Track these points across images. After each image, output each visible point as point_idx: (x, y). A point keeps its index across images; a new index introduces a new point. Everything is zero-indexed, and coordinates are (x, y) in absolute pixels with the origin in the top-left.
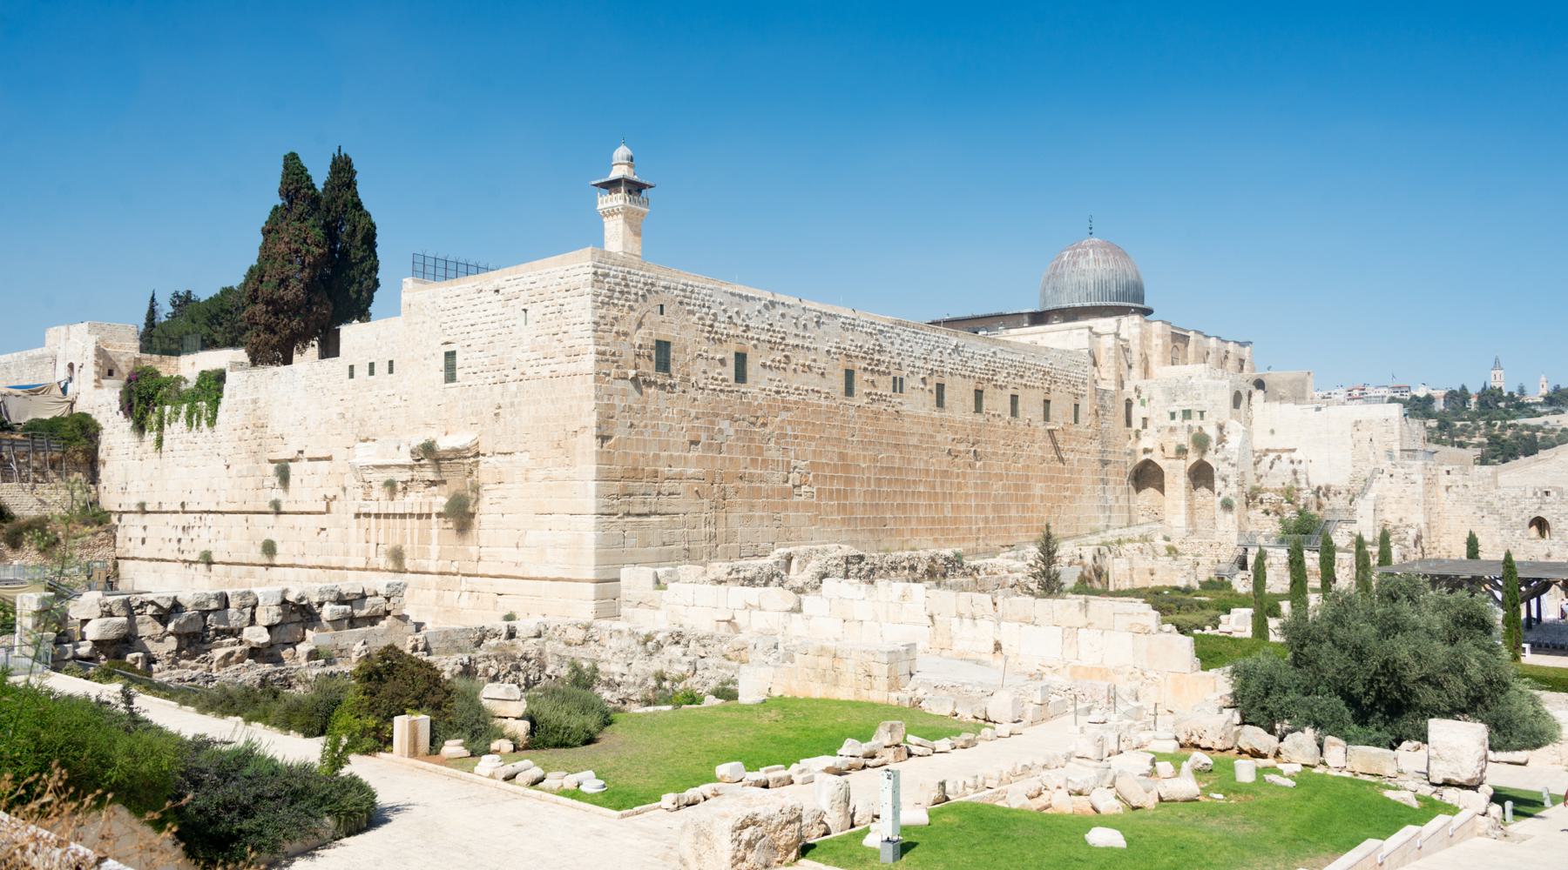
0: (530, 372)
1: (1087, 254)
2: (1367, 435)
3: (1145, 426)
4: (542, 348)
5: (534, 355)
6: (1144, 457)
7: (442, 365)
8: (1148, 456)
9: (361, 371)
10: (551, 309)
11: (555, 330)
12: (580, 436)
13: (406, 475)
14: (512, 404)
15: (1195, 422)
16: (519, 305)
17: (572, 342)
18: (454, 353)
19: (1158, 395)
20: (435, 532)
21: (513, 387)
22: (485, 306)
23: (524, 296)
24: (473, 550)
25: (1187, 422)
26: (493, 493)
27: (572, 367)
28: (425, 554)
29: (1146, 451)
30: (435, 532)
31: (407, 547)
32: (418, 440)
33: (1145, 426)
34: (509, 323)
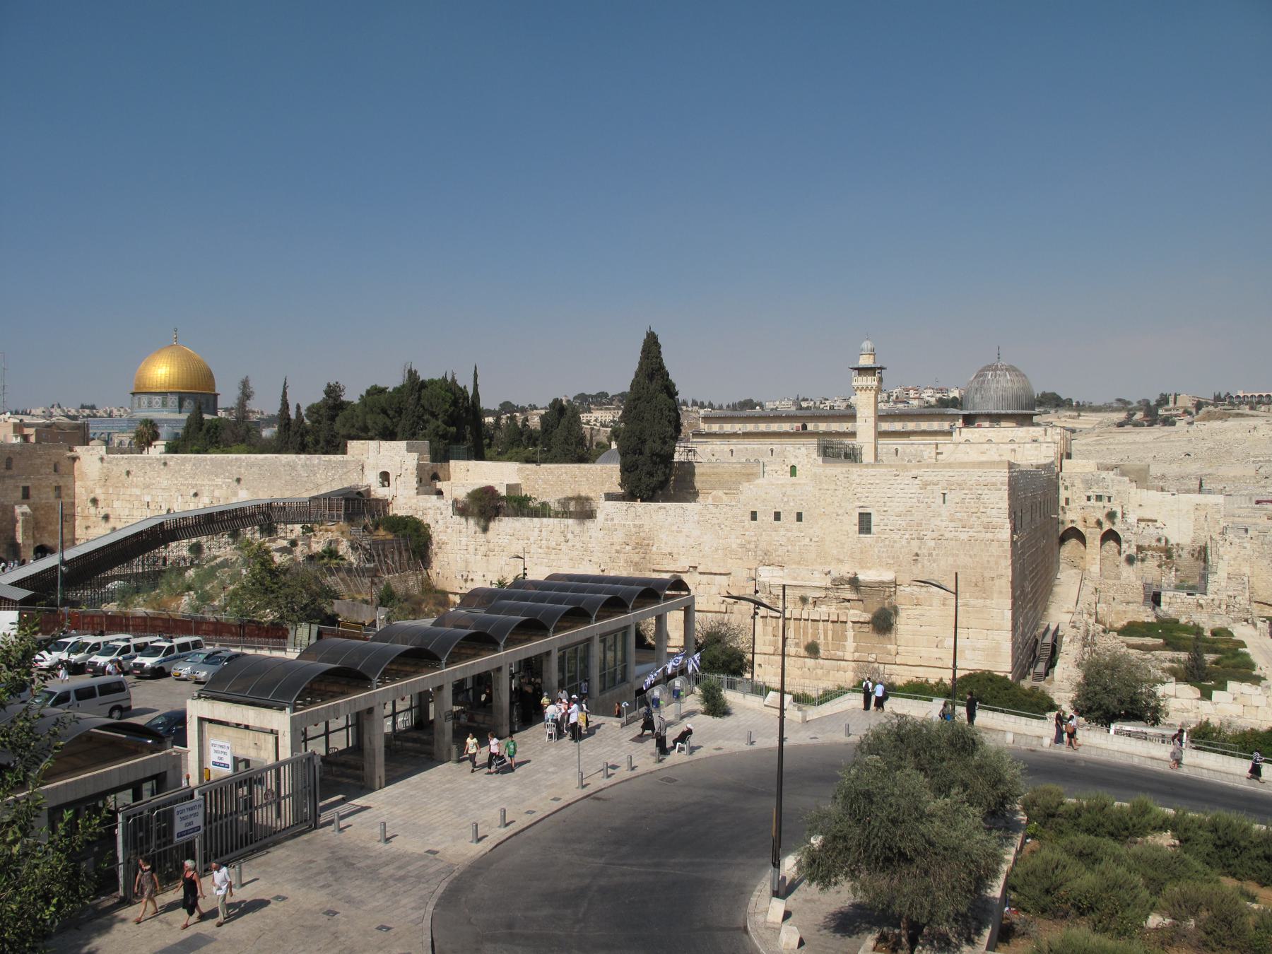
0: (947, 535)
3: (1067, 503)
5: (952, 524)
7: (857, 521)
9: (766, 518)
12: (997, 582)
13: (823, 594)
14: (930, 555)
16: (939, 491)
19: (1078, 482)
20: (850, 634)
21: (932, 543)
24: (892, 648)
25: (1100, 504)
26: (909, 612)
27: (989, 536)
28: (844, 648)
29: (1072, 521)
30: (850, 634)
31: (821, 641)
32: (846, 570)
33: (1067, 503)
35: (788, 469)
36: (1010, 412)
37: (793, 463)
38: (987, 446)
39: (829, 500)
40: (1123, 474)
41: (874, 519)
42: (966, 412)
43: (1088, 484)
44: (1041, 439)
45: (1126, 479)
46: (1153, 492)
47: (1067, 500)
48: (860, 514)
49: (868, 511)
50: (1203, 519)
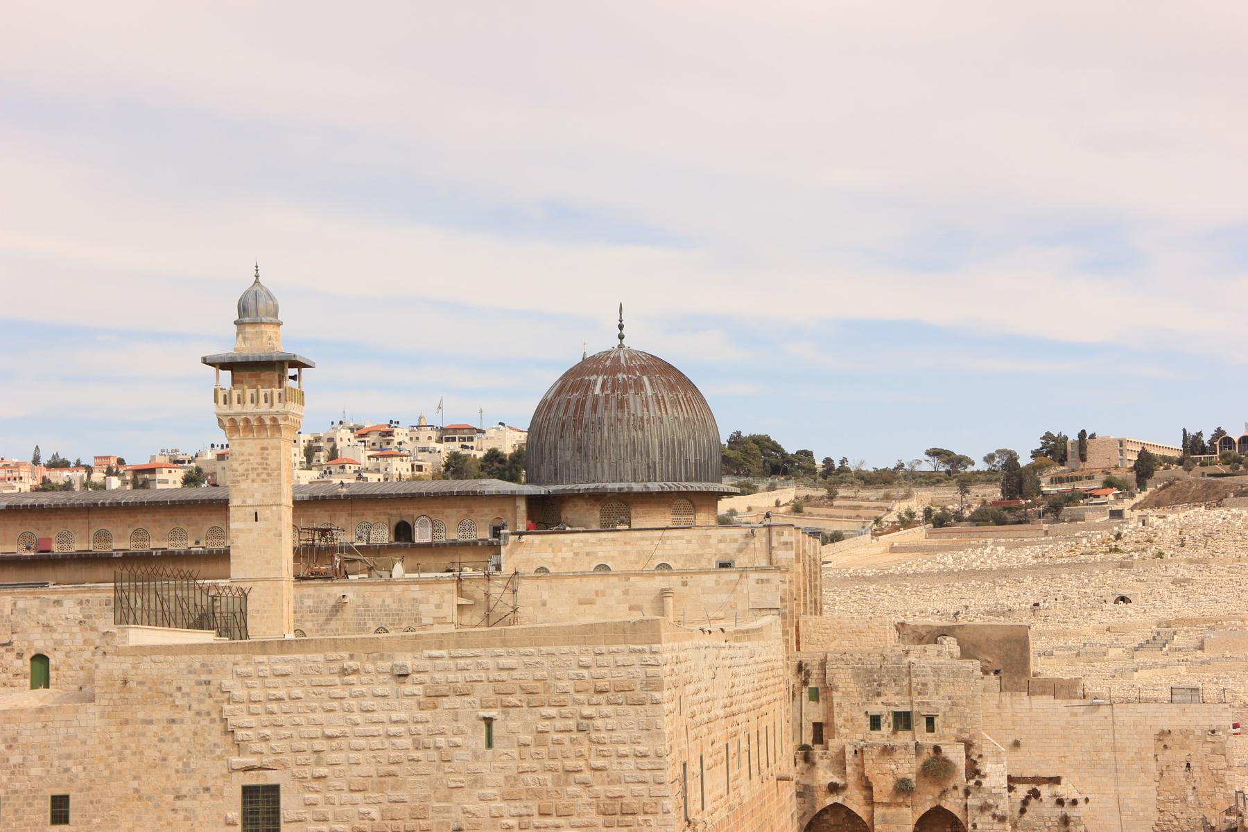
1: (639, 386)
2: (1182, 756)
3: (819, 737)
4: (536, 794)
6: (830, 801)
8: (839, 799)
10: (559, 724)
11: (570, 764)
15: (921, 734)
16: (470, 709)
17: (617, 789)
18: (276, 788)
22: (367, 703)
23: (484, 691)
25: (904, 737)
29: (833, 788)
34: (441, 741)
35: (25, 665)
36: (654, 486)
37: (40, 644)
38: (596, 584)
39: (152, 754)
40: (966, 654)
41: (289, 805)
42: (541, 490)
43: (873, 681)
44: (741, 561)
45: (974, 665)
46: (1042, 702)
47: (818, 728)
48: (248, 791)
49: (270, 778)
50: (1180, 771)
